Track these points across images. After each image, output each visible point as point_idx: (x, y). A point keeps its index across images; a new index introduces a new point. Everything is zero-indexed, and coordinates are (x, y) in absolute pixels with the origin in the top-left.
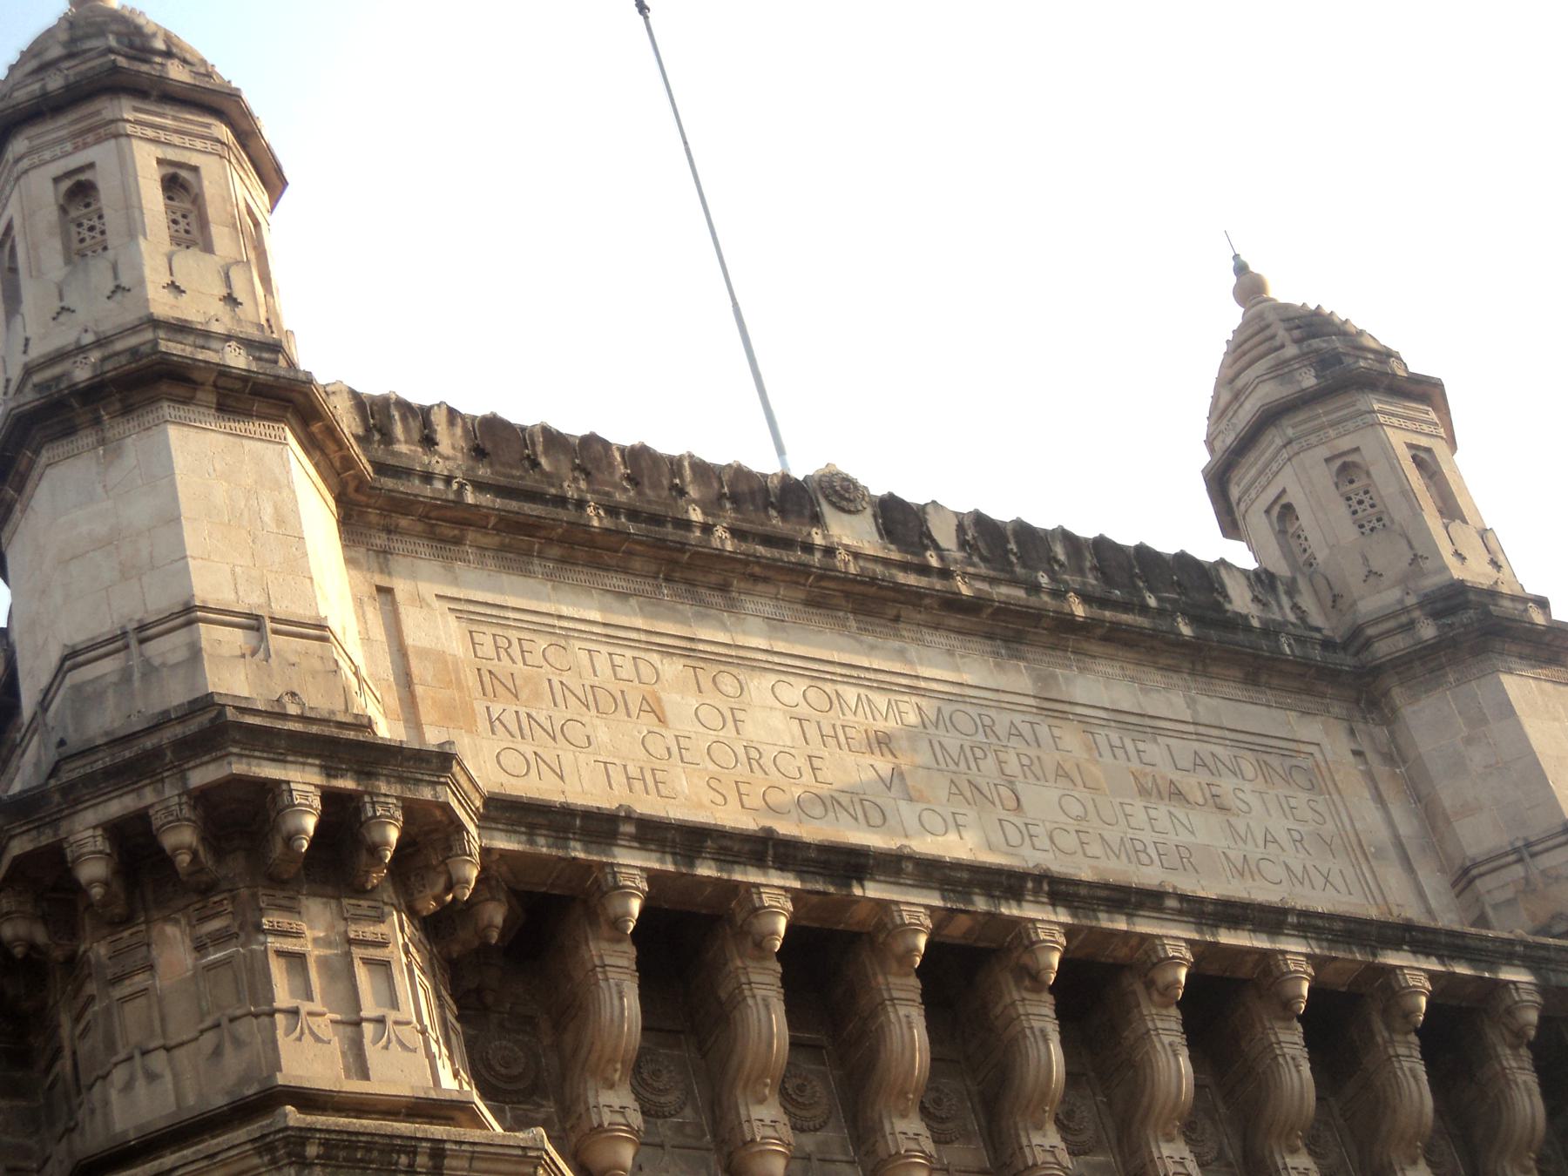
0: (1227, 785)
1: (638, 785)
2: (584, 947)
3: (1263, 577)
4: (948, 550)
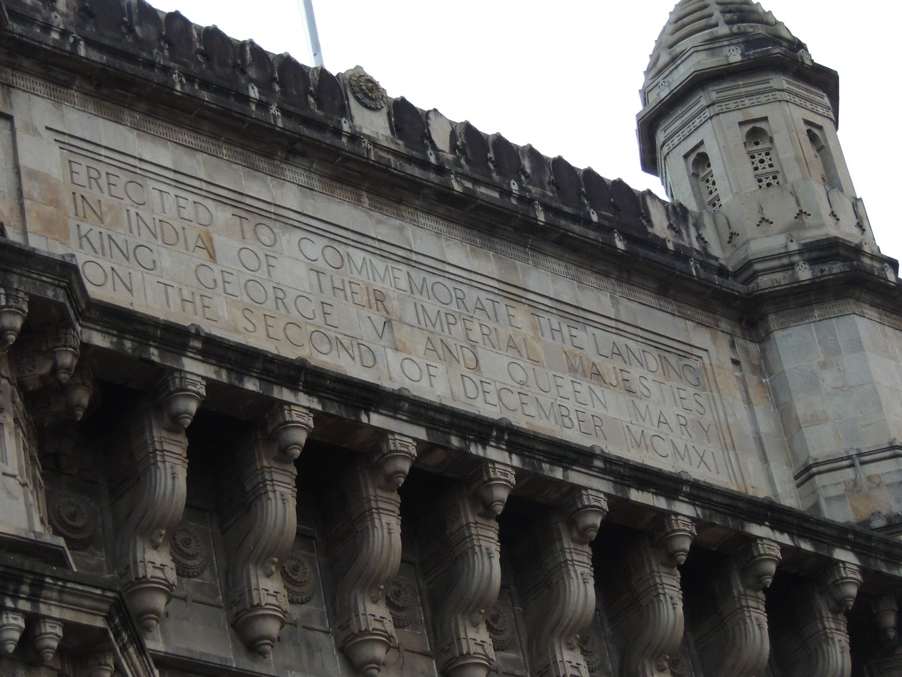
0: (635, 372)
2: (148, 433)
3: (678, 210)
4: (443, 151)
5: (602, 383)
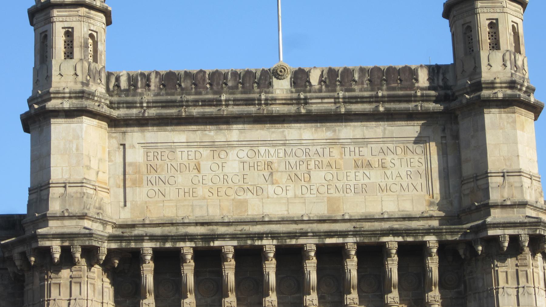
1: (187, 194)
4: (314, 86)
5: (371, 168)
